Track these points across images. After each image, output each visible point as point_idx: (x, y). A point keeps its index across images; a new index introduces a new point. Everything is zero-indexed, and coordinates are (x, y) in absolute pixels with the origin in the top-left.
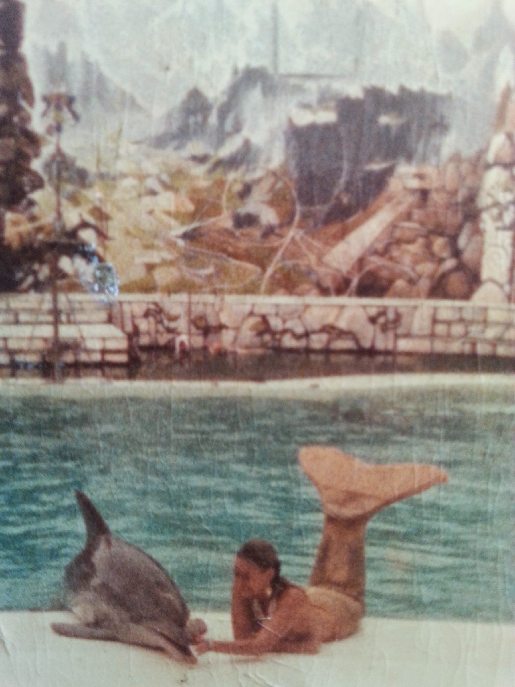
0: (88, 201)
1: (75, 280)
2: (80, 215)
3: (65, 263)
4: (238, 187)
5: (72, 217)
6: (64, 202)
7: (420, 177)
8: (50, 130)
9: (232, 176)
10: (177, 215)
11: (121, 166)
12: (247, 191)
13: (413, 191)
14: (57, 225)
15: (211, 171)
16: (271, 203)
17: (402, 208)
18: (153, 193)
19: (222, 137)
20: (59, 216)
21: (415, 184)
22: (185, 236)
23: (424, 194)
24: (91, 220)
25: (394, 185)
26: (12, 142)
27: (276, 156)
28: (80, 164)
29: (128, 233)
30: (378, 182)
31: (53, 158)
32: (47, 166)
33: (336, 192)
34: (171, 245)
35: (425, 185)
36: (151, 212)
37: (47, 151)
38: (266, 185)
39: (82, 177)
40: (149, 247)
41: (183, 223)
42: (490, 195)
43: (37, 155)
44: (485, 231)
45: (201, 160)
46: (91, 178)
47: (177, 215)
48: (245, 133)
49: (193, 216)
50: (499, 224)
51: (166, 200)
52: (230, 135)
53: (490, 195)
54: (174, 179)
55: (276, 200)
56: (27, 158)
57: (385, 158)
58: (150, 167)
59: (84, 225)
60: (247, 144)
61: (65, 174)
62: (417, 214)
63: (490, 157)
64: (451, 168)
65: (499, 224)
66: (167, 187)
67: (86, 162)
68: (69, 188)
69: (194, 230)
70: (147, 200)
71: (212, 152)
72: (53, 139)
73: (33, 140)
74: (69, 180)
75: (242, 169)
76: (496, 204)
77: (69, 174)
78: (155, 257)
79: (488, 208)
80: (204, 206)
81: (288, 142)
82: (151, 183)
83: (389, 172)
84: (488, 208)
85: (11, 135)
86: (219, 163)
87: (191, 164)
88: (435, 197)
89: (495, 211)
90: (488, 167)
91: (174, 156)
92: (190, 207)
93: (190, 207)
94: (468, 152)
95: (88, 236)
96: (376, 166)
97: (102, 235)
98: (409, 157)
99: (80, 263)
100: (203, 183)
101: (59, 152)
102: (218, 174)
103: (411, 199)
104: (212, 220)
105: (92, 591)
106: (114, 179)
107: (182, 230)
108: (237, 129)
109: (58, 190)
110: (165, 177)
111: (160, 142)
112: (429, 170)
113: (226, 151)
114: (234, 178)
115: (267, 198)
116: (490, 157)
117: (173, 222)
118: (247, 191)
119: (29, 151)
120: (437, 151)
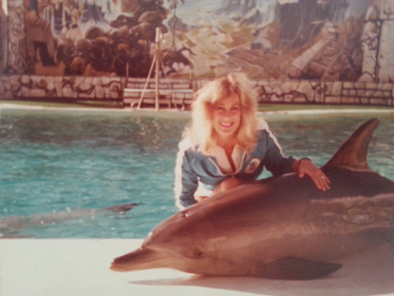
0: (186, 38)
1: (180, 73)
2: (183, 45)
3: (175, 66)
4: (253, 31)
5: (179, 45)
6: (176, 38)
7: (335, 27)
8: (171, 8)
9: (252, 26)
10: (224, 44)
11: (202, 23)
12: (257, 34)
13: (332, 33)
14: (173, 50)
15: (241, 24)
16: (268, 39)
17: (327, 41)
18: (215, 34)
19: (247, 9)
20: (174, 44)
21: (333, 30)
22: (229, 54)
23: (337, 35)
24: (187, 46)
25: (324, 31)
26: (155, 12)
27: (270, 18)
28: (184, 22)
29: (203, 52)
30: (318, 29)
31: (172, 20)
32: (169, 23)
33: (298, 34)
34: (223, 57)
35: (338, 31)
36: (214, 43)
37: (170, 16)
38: (265, 31)
39: (184, 28)
40: (212, 58)
41: (228, 47)
42: (366, 34)
43: (165, 18)
44: (364, 51)
45: (238, 19)
46: (189, 28)
47: (224, 44)
48: (257, 7)
49: (233, 44)
50: (370, 47)
51: (221, 37)
52: (250, 8)
53: (366, 34)
54: (225, 28)
55: (270, 38)
56: (161, 20)
57: (320, 19)
58: (215, 23)
59: (184, 49)
60: (258, 12)
61: (177, 26)
62: (334, 44)
63: (367, 18)
64: (349, 24)
65: (370, 47)
66: (221, 31)
67: (189, 21)
68: (178, 32)
69: (233, 50)
70: (212, 37)
71: (241, 16)
72: (173, 11)
73: (164, 12)
74: (178, 29)
75: (256, 23)
76: (369, 38)
77: (178, 25)
78: (215, 63)
79: (365, 40)
80: (237, 41)
81: (276, 11)
82: (215, 30)
83: (322, 25)
84: (365, 40)
85: (155, 9)
86: (246, 20)
87: (233, 21)
88: (341, 36)
89: (368, 41)
90: (365, 22)
91: (226, 18)
92: (232, 40)
93: (232, 40)
94: (357, 16)
95: (185, 53)
96: (317, 22)
97: (191, 53)
98: (330, 19)
99: (182, 65)
100: (237, 30)
101: (175, 17)
102: (244, 25)
103: (331, 37)
104: (242, 46)
105: (230, 191)
106: (198, 28)
107: (227, 50)
108: (254, 6)
109: (174, 33)
110: (221, 27)
111: (219, 12)
112: (339, 24)
113: (249, 15)
114: (253, 27)
115: (267, 36)
116: (367, 18)
117: (222, 47)
118: (257, 34)
119: (162, 16)
120: (343, 16)
